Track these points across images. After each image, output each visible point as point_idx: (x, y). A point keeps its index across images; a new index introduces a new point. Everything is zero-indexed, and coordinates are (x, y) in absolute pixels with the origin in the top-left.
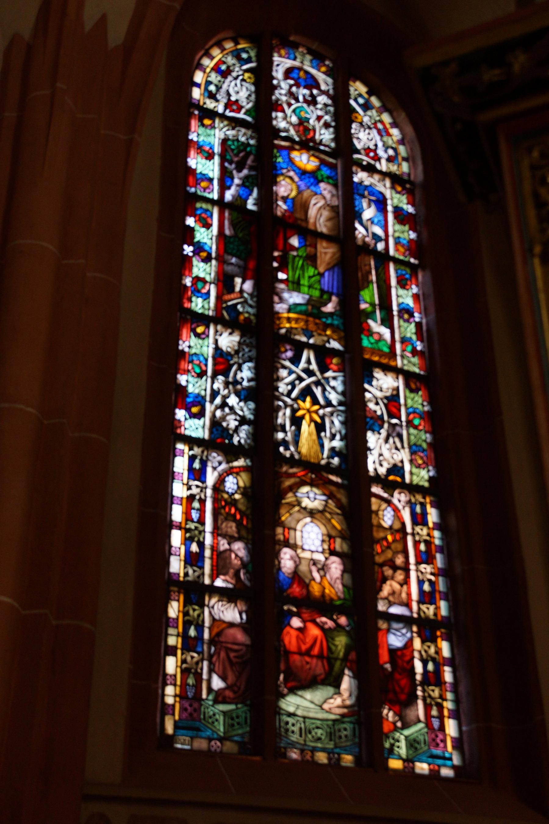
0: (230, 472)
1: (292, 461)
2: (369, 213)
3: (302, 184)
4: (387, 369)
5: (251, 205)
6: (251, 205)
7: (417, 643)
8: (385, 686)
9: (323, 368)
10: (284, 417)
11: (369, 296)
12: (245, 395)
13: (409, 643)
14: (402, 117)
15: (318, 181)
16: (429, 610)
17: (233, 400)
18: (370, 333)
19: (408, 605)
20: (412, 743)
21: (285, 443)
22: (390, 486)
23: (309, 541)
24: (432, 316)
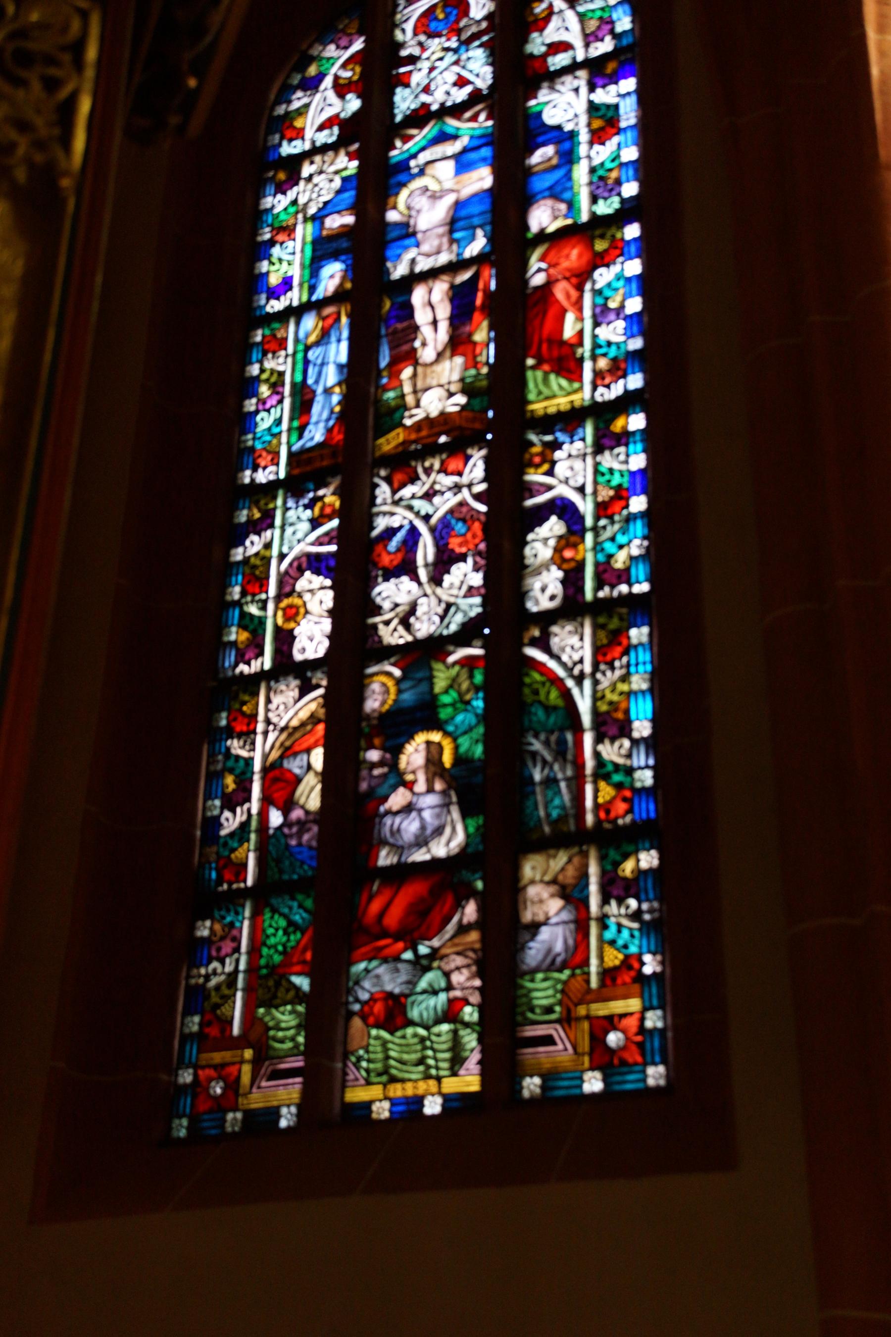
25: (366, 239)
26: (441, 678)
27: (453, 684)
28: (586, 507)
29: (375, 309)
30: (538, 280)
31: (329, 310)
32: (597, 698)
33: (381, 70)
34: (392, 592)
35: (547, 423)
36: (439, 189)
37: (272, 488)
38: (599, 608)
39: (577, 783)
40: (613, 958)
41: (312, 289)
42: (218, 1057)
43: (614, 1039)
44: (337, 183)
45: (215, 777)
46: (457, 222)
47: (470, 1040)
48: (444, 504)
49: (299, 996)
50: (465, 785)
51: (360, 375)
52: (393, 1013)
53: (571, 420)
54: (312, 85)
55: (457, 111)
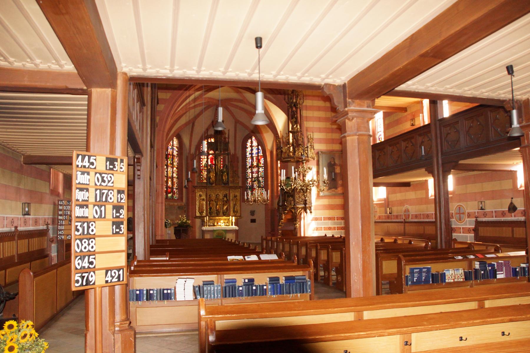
8: (174, 193)
23: (170, 183)
25: (251, 154)
29: (252, 158)
33: (252, 143)
34: (254, 175)
36: (255, 151)
51: (252, 162)
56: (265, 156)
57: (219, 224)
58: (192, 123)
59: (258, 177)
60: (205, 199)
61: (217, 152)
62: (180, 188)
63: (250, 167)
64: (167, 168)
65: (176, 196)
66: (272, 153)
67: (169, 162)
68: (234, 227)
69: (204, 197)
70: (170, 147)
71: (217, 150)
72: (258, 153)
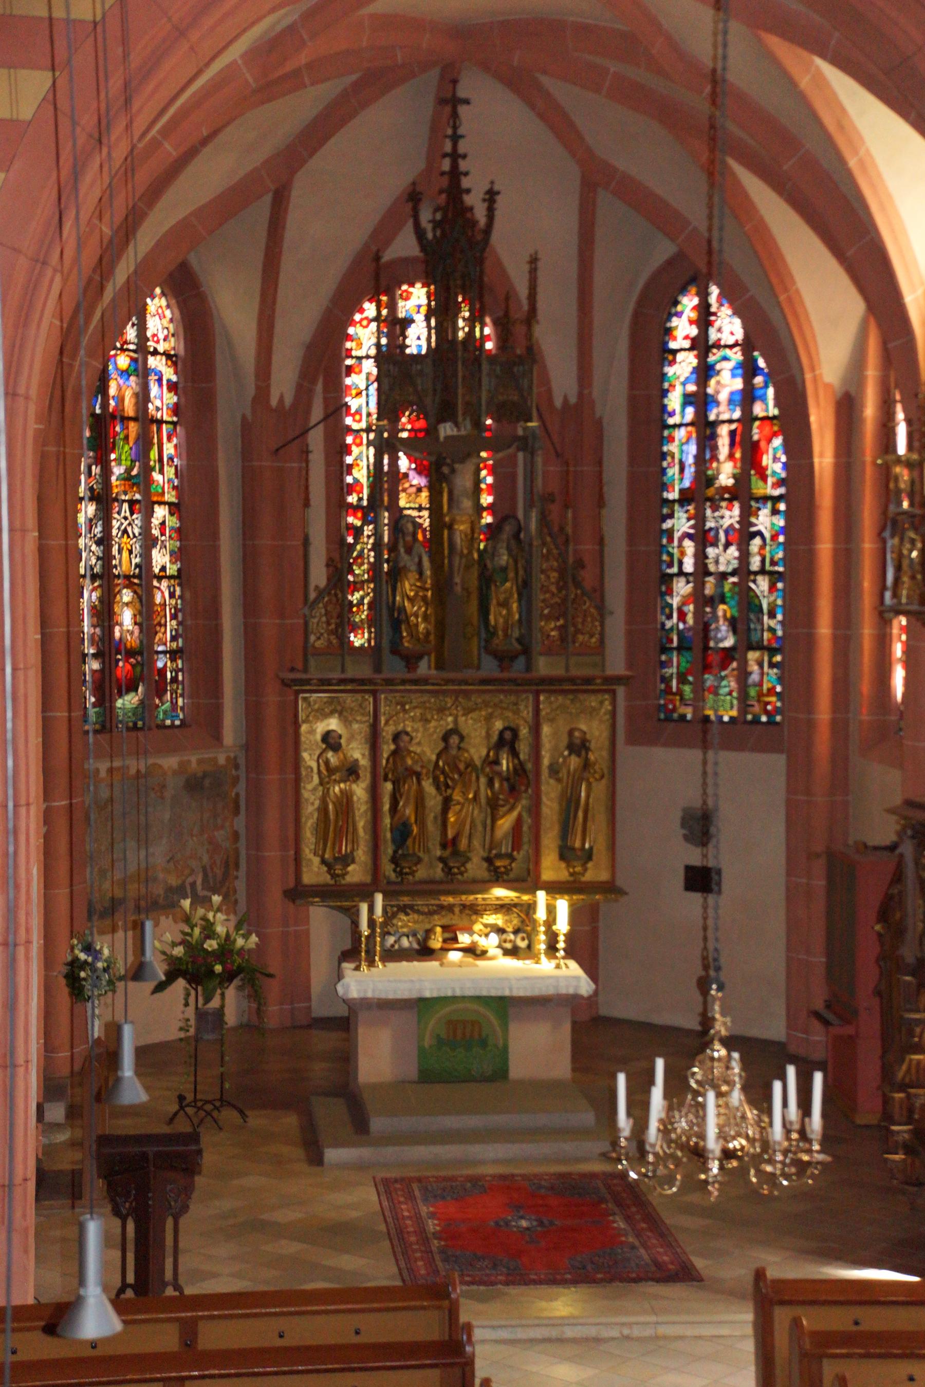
0: (92, 591)
1: (118, 577)
2: (154, 390)
3: (121, 382)
4: (160, 503)
5: (98, 411)
6: (98, 411)
7: (169, 664)
9: (132, 514)
10: (115, 550)
11: (154, 454)
12: (99, 543)
13: (165, 665)
14: (173, 302)
15: (129, 376)
16: (174, 645)
17: (94, 548)
18: (153, 482)
19: (165, 644)
20: (165, 712)
21: (116, 567)
22: (160, 579)
24: (185, 462)
25: (700, 400)
26: (727, 587)
27: (730, 590)
28: (767, 535)
29: (705, 431)
30: (756, 438)
31: (689, 428)
32: (769, 604)
33: (704, 318)
34: (711, 552)
35: (757, 500)
37: (674, 501)
38: (771, 573)
39: (763, 630)
40: (770, 685)
41: (683, 417)
42: (671, 697)
43: (769, 707)
44: (690, 369)
45: (663, 608)
46: (730, 402)
47: (735, 702)
48: (726, 523)
49: (690, 683)
50: (733, 624)
51: (700, 459)
52: (715, 691)
53: (765, 499)
54: (679, 315)
55: (731, 347)
56: (793, 424)
57: (464, 939)
58: (272, 189)
59: (743, 570)
60: (364, 762)
61: (446, 430)
62: (199, 647)
63: (686, 498)
64: (104, 515)
65: (173, 706)
66: (847, 407)
67: (118, 471)
68: (569, 975)
69: (358, 752)
70: (123, 361)
71: (447, 412)
72: (748, 396)
